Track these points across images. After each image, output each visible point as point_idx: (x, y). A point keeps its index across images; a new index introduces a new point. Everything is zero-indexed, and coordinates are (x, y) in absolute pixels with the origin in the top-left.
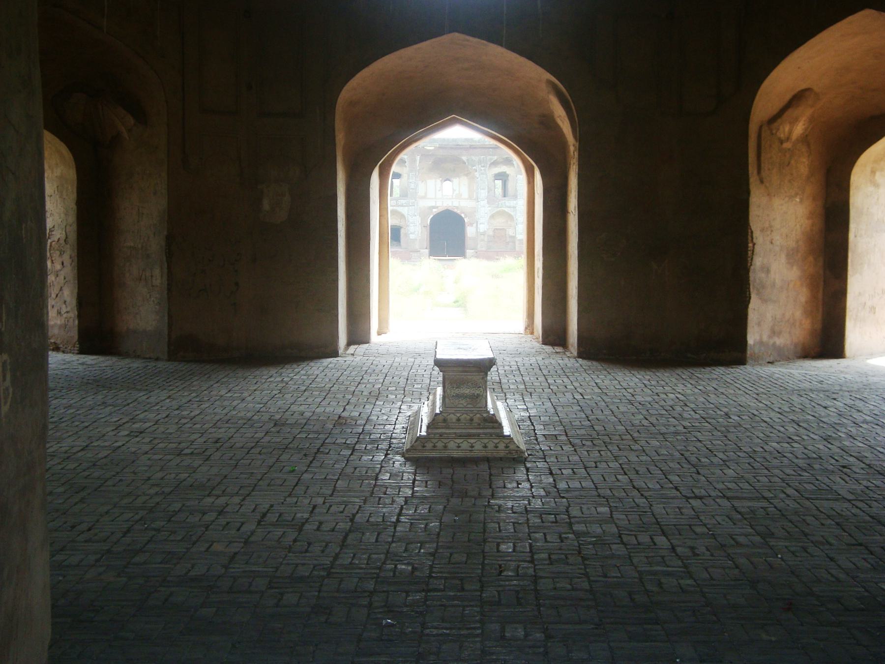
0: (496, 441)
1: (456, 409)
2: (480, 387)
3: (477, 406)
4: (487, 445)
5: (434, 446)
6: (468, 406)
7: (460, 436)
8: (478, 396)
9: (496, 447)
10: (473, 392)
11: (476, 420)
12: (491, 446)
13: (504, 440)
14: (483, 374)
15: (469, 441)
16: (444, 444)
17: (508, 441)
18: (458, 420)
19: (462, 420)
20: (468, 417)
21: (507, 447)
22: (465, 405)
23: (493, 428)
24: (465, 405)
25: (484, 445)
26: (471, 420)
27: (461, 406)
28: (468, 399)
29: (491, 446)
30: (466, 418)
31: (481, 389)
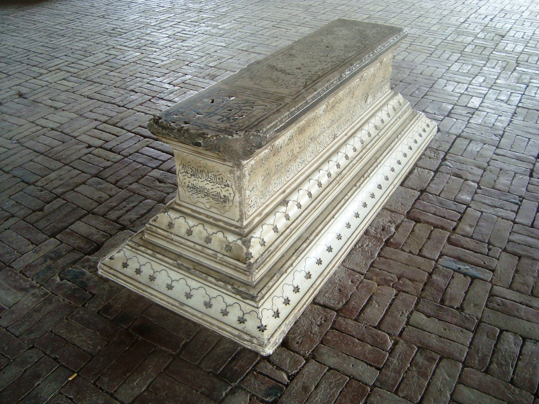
0: (230, 300)
1: (194, 208)
2: (228, 186)
3: (225, 215)
4: (213, 301)
5: (138, 271)
6: (213, 210)
7: (179, 266)
8: (225, 200)
9: (225, 313)
10: (218, 190)
11: (215, 245)
12: (218, 306)
13: (241, 303)
14: (231, 164)
15: (190, 281)
16: (151, 273)
17: (250, 308)
18: (189, 232)
19: (194, 233)
20: (205, 234)
21: (242, 321)
22: (208, 206)
23: (236, 268)
24: (208, 206)
25: (207, 299)
26: (208, 240)
27: (202, 206)
28: (211, 200)
29: (218, 306)
30: (201, 232)
31: (230, 189)
